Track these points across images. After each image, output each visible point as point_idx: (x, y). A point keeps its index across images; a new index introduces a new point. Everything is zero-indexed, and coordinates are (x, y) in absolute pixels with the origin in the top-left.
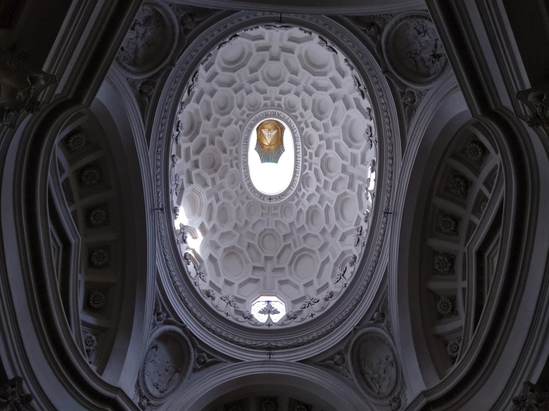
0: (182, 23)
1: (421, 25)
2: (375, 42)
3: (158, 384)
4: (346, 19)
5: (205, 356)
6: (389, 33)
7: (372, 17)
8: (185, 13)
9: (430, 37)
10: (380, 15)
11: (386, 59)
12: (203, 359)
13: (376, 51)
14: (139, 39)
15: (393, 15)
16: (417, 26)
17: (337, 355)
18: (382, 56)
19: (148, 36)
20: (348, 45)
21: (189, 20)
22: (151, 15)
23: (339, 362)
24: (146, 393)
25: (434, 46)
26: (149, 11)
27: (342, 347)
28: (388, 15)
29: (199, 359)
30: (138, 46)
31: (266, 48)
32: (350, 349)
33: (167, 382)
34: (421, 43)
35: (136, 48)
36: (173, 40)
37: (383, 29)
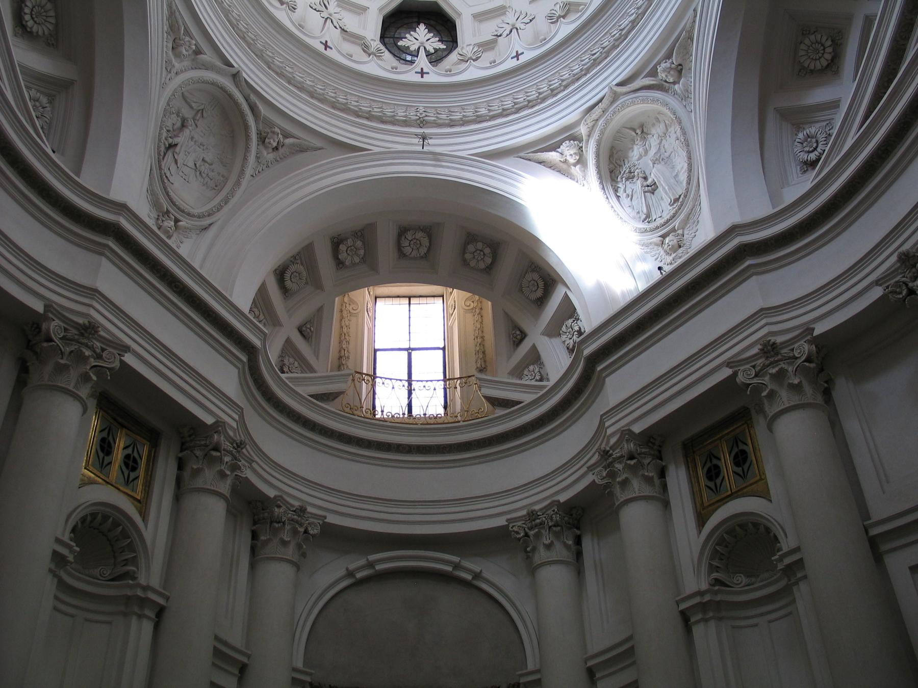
0: (582, 151)
1: (204, 175)
6: (247, 149)
10: (268, 166)
13: (260, 107)
18: (247, 99)
26: (625, 191)
28: (257, 172)
30: (658, 141)
34: (193, 143)
35: (662, 140)
37: (258, 145)
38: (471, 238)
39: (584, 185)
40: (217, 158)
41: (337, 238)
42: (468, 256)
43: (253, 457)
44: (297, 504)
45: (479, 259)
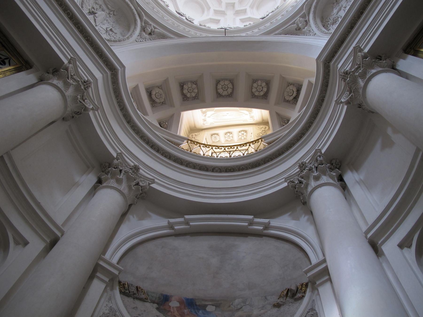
0: (307, 22)
1: (111, 36)
2: (145, 20)
4: (172, 36)
6: (135, 28)
7: (152, 39)
8: (303, 30)
9: (101, 27)
11: (133, 8)
14: (344, 6)
15: (136, 42)
16: (115, 35)
19: (336, 9)
20: (167, 17)
21: (300, 25)
22: (331, 26)
25: (96, 20)
28: (139, 41)
31: (238, 13)
36: (316, 7)
38: (255, 81)
39: (310, 35)
40: (120, 33)
41: (183, 83)
42: (254, 90)
43: (95, 101)
44: (132, 163)
45: (260, 90)
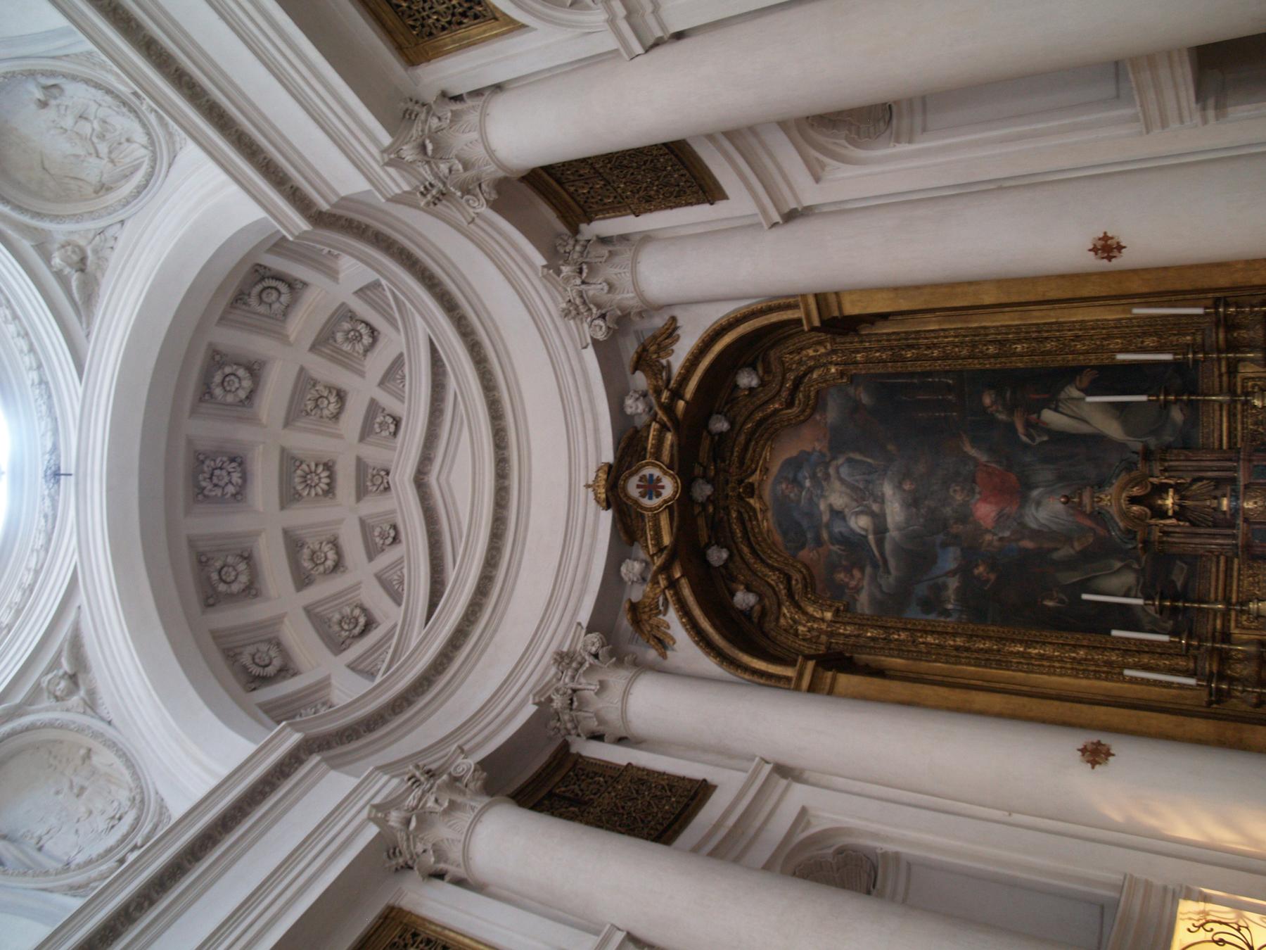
3: (112, 815)
5: (50, 676)
12: (58, 684)
17: (53, 263)
23: (75, 258)
24: (111, 858)
27: (26, 245)
29: (58, 693)
32: (25, 219)
33: (113, 788)
